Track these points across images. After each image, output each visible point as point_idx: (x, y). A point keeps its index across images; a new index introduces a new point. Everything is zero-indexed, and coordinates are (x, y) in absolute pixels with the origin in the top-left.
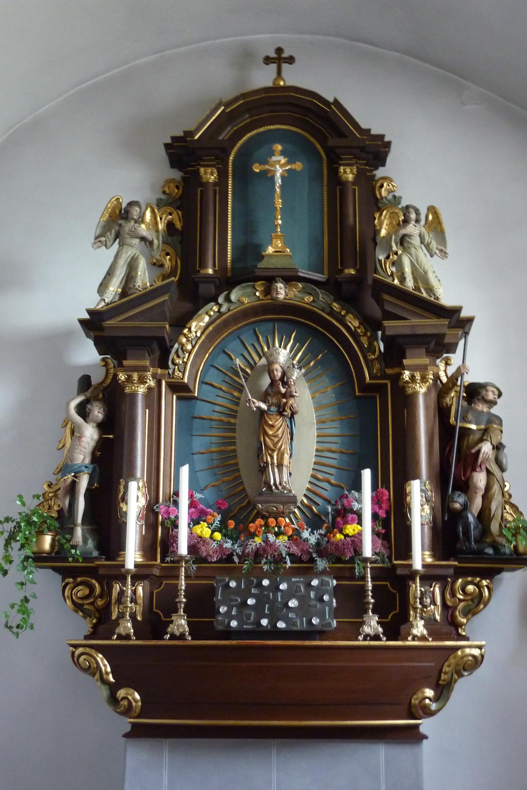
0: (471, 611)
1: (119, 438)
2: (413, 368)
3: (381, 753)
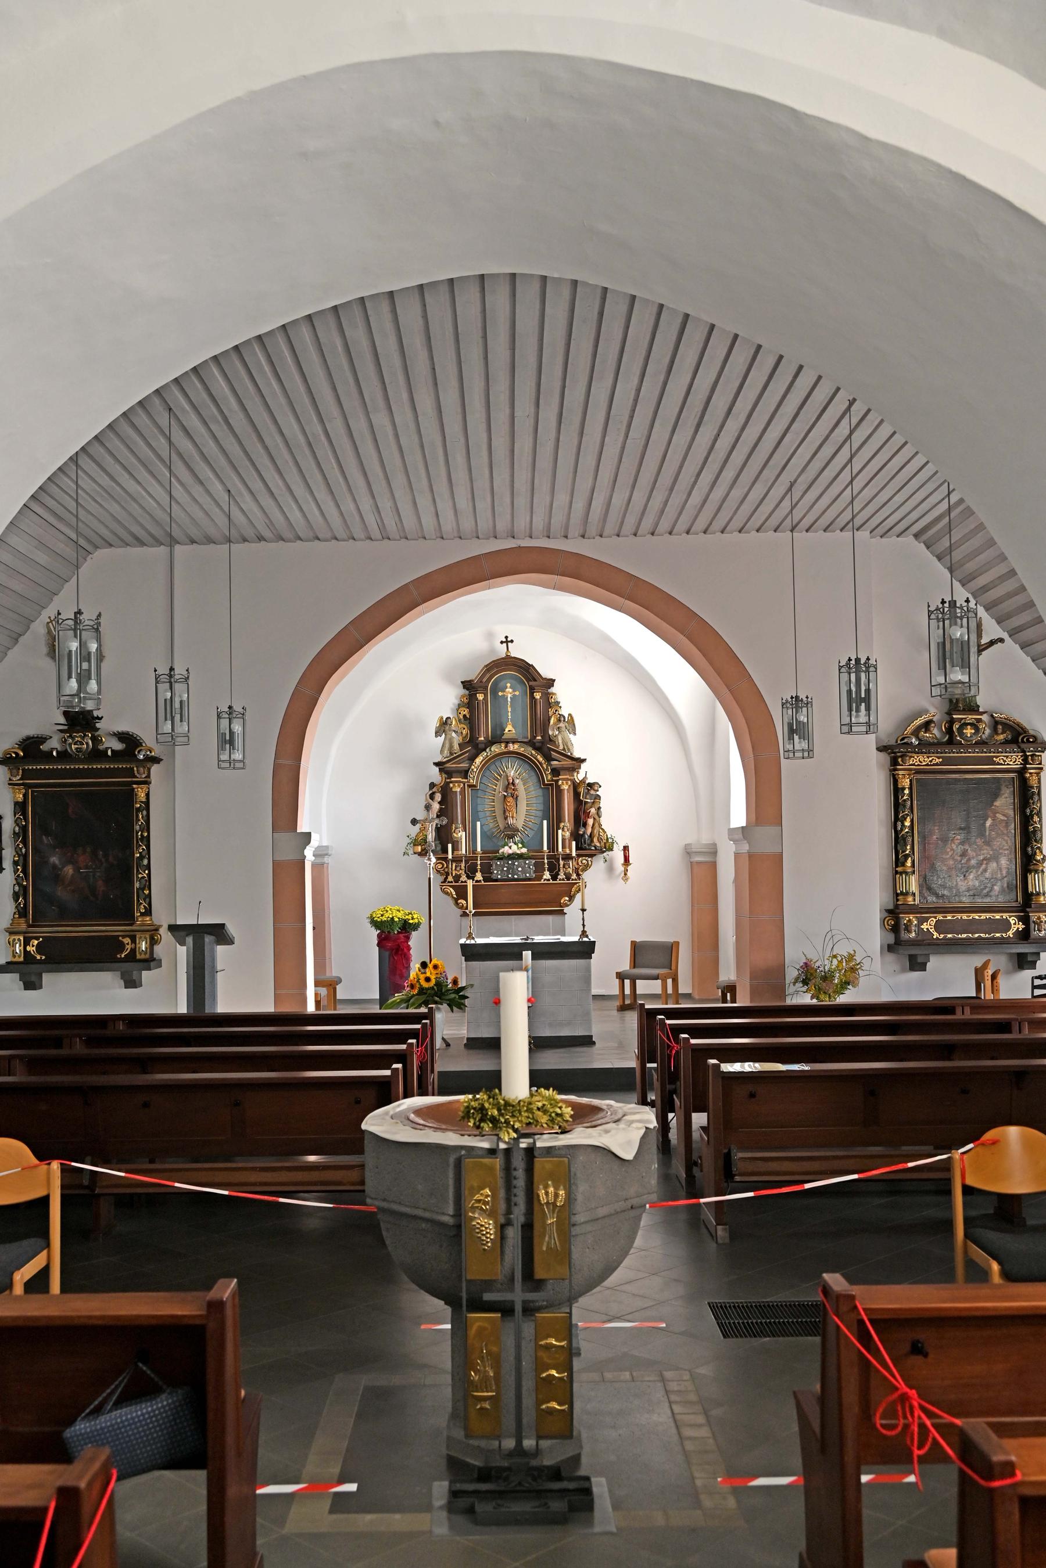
0: (584, 870)
1: (446, 807)
2: (563, 779)
3: (550, 918)
